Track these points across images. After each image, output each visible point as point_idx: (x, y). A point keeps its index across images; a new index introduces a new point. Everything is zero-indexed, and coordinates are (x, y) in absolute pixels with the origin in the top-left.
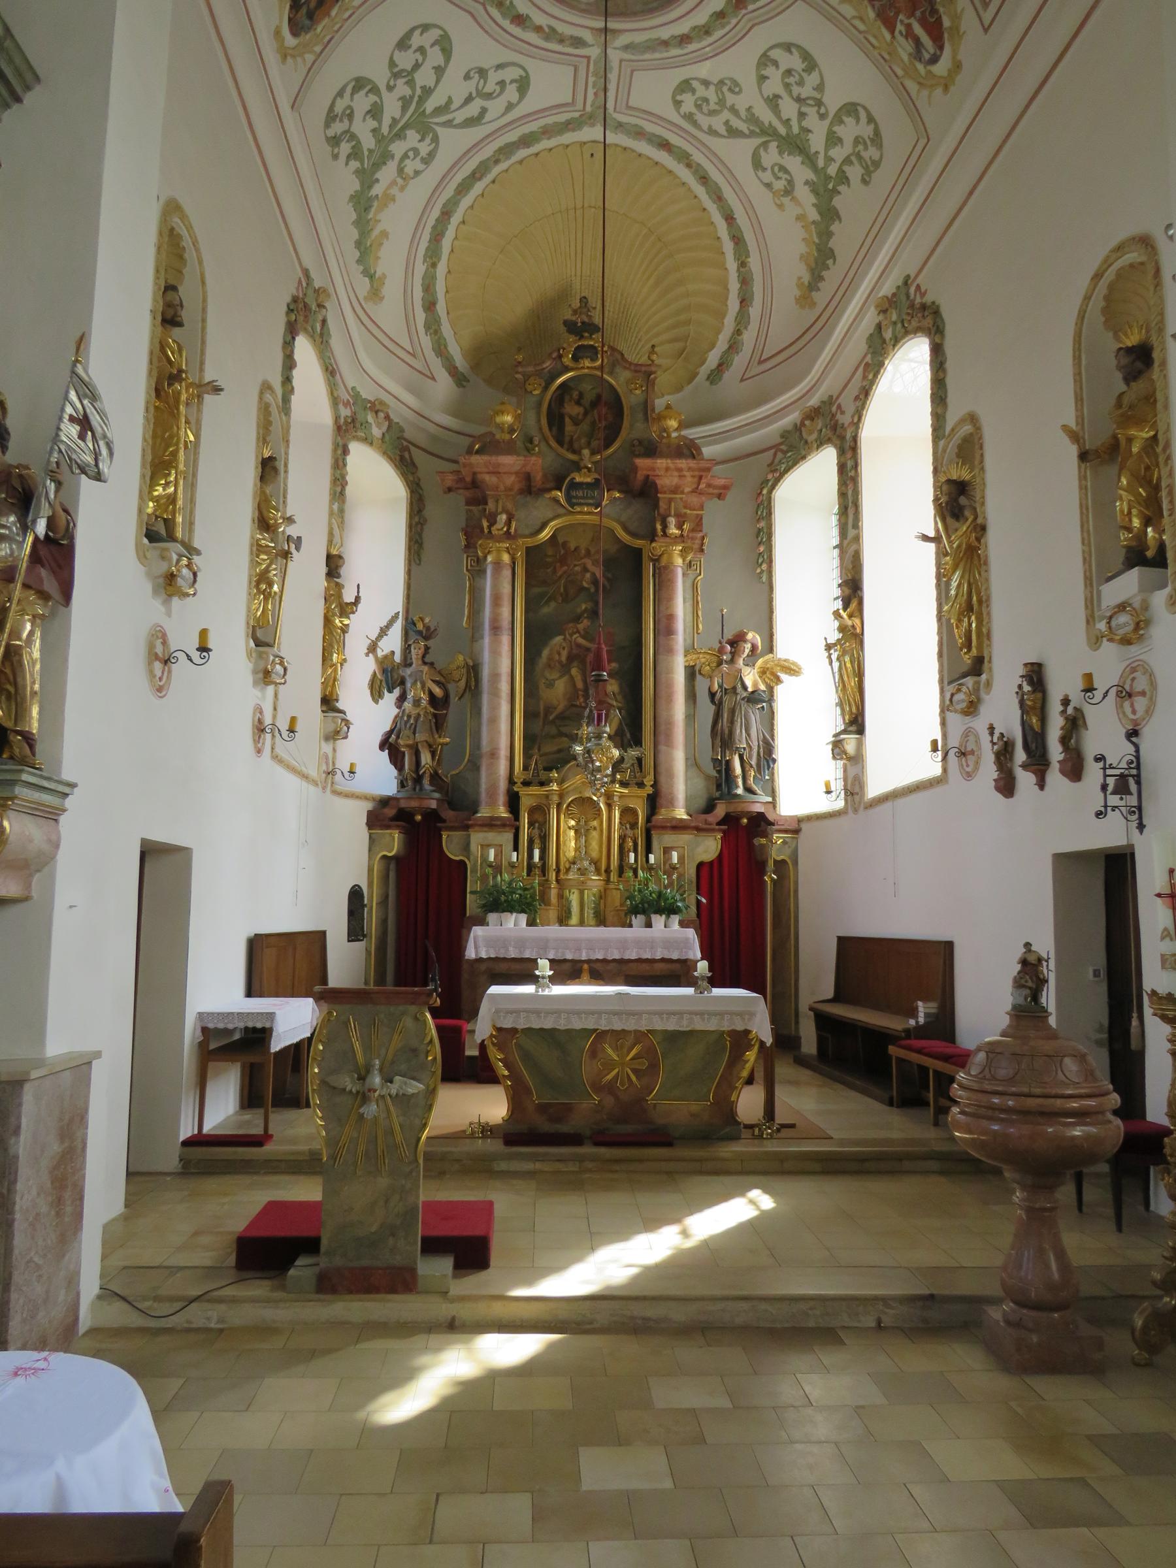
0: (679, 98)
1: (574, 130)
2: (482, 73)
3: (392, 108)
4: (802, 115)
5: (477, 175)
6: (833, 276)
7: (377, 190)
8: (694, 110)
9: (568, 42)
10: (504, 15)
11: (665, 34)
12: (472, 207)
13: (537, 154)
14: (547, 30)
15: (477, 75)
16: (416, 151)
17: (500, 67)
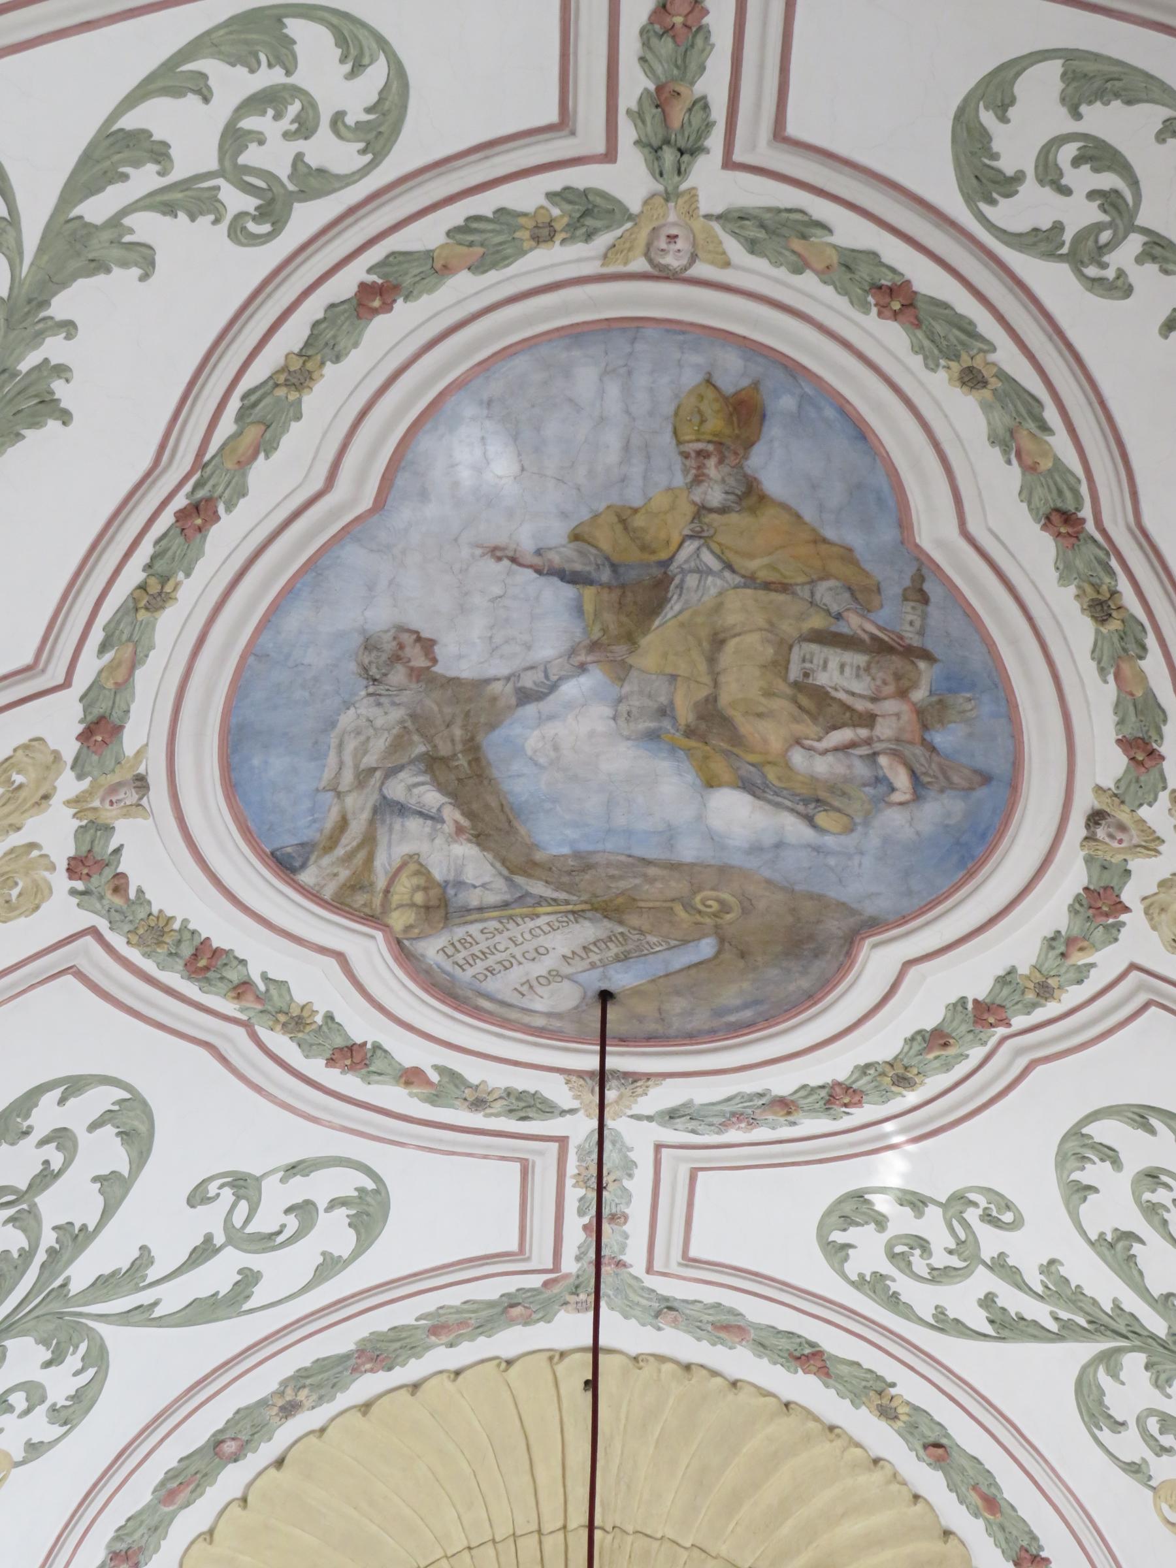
0: (838, 1237)
1: (527, 1321)
5: (229, 1447)
8: (887, 1268)
9: (498, 1106)
10: (307, 1049)
11: (782, 1082)
12: (209, 1535)
13: (415, 1387)
14: (434, 1077)
15: (228, 1195)
16: (35, 1393)
17: (293, 1169)
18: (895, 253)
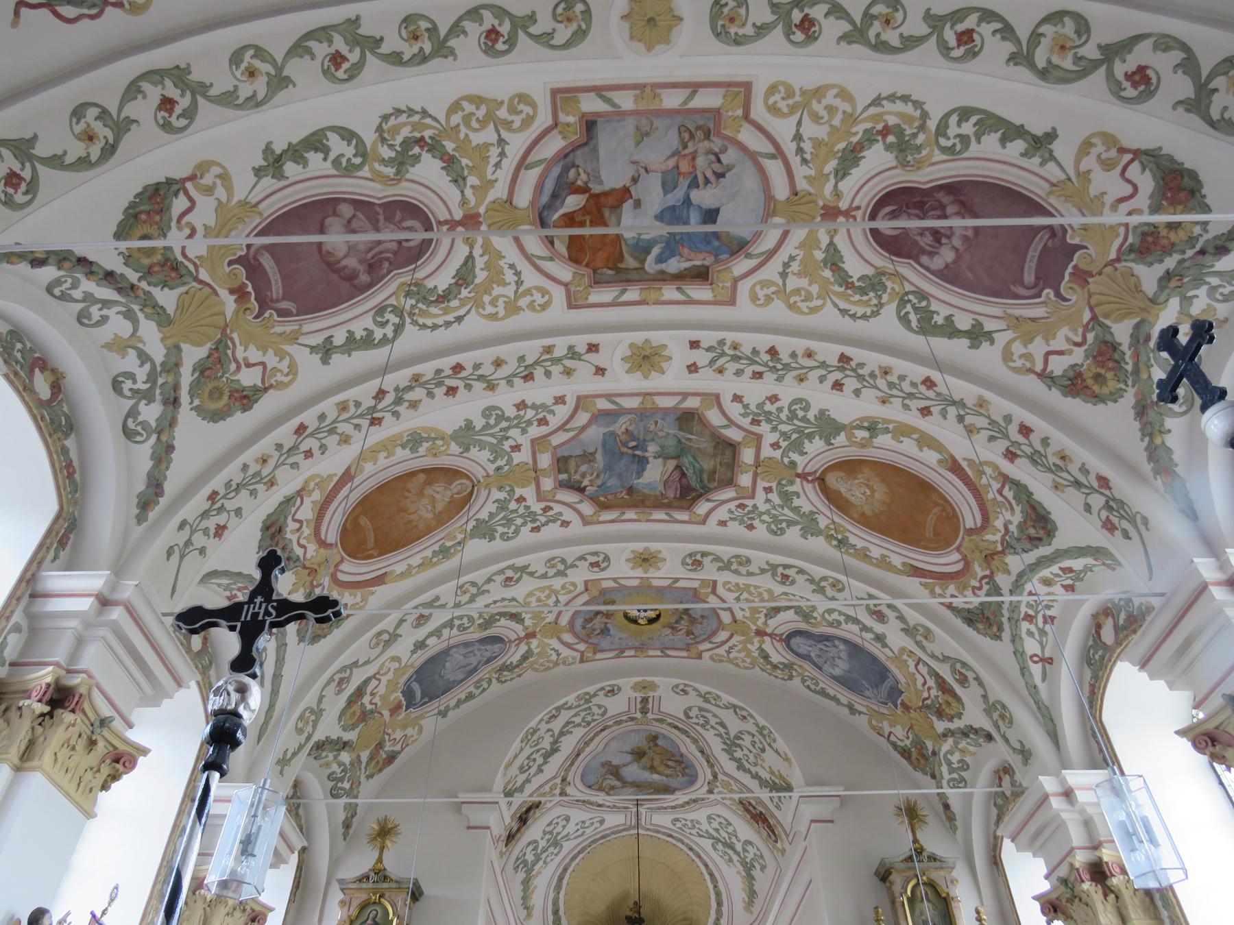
2: (583, 822)
3: (542, 844)
4: (730, 838)
6: (758, 903)
7: (534, 873)
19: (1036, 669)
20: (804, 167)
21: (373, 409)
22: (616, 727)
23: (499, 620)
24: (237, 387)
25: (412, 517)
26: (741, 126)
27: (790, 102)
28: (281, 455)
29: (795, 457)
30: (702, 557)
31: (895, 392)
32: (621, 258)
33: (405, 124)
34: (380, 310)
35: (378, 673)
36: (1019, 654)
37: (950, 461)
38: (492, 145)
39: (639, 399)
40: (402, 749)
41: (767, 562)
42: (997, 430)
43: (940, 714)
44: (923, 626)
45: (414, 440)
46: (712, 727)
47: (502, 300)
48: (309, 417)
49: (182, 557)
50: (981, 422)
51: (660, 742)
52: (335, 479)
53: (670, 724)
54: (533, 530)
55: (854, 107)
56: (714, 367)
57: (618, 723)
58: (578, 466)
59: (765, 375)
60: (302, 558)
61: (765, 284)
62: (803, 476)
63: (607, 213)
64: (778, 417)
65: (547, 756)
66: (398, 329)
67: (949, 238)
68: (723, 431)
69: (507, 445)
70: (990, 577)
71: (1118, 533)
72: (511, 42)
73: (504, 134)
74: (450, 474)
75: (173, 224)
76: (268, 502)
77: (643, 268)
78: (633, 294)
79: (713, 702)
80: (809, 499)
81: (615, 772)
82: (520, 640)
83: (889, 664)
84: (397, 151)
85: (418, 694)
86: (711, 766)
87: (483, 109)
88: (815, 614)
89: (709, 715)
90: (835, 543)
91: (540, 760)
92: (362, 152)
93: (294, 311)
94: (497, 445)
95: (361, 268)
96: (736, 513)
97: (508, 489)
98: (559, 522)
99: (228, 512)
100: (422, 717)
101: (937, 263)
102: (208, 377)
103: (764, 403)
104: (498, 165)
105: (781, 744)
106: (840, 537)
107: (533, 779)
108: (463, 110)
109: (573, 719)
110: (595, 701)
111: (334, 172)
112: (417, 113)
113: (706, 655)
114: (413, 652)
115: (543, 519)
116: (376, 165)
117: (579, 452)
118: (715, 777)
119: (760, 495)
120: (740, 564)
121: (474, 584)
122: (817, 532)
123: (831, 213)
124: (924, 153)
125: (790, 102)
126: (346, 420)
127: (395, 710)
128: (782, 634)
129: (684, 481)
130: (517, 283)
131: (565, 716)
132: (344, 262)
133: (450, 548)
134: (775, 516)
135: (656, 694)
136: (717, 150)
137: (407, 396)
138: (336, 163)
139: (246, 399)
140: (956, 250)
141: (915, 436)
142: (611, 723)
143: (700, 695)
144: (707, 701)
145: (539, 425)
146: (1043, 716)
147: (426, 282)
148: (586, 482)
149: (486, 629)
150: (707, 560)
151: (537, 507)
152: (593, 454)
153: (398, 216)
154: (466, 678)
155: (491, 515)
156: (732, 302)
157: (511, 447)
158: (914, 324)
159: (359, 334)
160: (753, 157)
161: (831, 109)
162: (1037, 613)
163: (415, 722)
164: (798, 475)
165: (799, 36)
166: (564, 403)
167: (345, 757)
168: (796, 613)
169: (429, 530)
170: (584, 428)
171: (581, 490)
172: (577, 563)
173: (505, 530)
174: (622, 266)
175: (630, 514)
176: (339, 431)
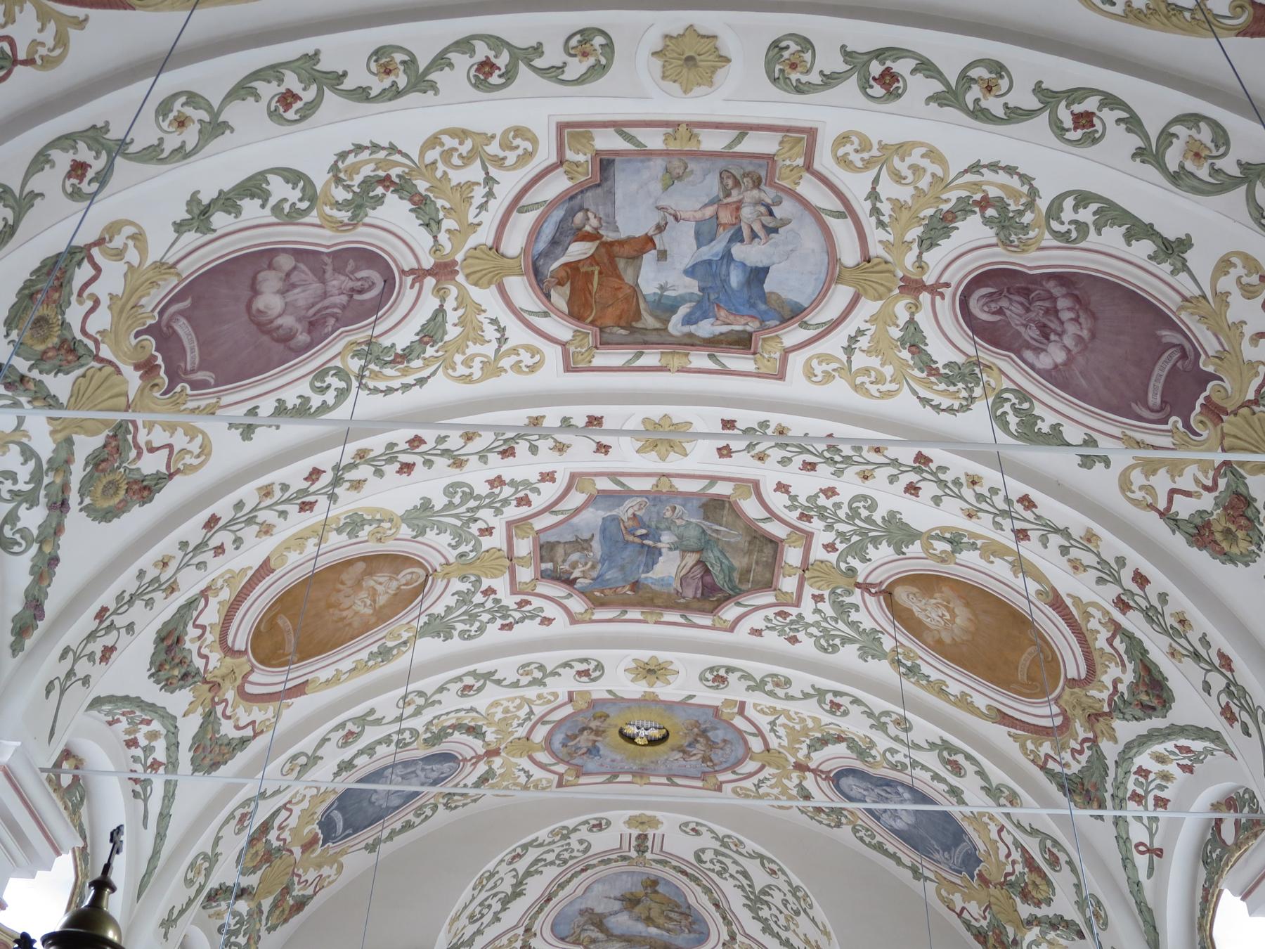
18: (683, 867)
19: (1141, 861)
20: (880, 230)
21: (305, 492)
22: (602, 867)
23: (452, 734)
24: (137, 477)
25: (345, 613)
26: (801, 177)
27: (866, 155)
28: (187, 554)
29: (855, 563)
30: (727, 672)
31: (984, 506)
32: (638, 315)
33: (367, 162)
34: (321, 374)
35: (290, 802)
36: (1123, 840)
37: (1051, 594)
38: (478, 184)
39: (653, 480)
40: (315, 893)
41: (813, 686)
42: (1108, 572)
43: (1025, 896)
44: (1009, 788)
45: (354, 523)
46: (731, 876)
47: (478, 360)
48: (223, 507)
49: (62, 692)
50: (1088, 559)
51: (660, 888)
52: (250, 573)
53: (675, 868)
54: (503, 627)
55: (946, 168)
56: (753, 453)
57: (603, 862)
58: (567, 555)
59: (818, 467)
60: (202, 671)
61: (824, 358)
62: (865, 587)
63: (621, 264)
64: (835, 514)
65: (506, 902)
66: (342, 394)
67: (1060, 335)
68: (761, 525)
69: (474, 529)
70: (1094, 742)
71: (1237, 725)
72: (509, 75)
73: (494, 172)
74: (398, 561)
75: (74, 298)
76: (166, 609)
77: (666, 329)
78: (651, 358)
79: (735, 849)
80: (870, 614)
81: (598, 921)
82: (478, 758)
83: (965, 825)
84: (354, 192)
85: (340, 825)
86: (728, 923)
87: (468, 144)
88: (873, 752)
89: (728, 862)
90: (903, 670)
91: (497, 907)
92: (310, 194)
93: (212, 381)
94: (461, 528)
95: (299, 327)
96: (774, 621)
97: (473, 579)
98: (538, 619)
99: (118, 629)
100: (344, 852)
101: (1044, 361)
102: (103, 471)
103: (817, 496)
104: (483, 207)
105: (818, 912)
106: (909, 664)
107: (486, 930)
108: (442, 144)
109: (544, 857)
110: (574, 837)
111: (274, 220)
112: (383, 148)
113: (727, 788)
114: (336, 774)
115: (517, 615)
116: (327, 209)
117: (570, 538)
118: (733, 938)
119: (807, 605)
120: (777, 685)
121: (421, 694)
122: (880, 655)
123: (912, 287)
124: (1032, 234)
125: (866, 155)
126: (269, 507)
127: (308, 846)
128: (830, 771)
129: (708, 579)
130: (499, 340)
131: (533, 854)
132: (279, 321)
133: (391, 649)
134: (825, 630)
135: (659, 832)
136: (769, 201)
137: (348, 476)
138: (277, 209)
139: (145, 489)
140: (1069, 351)
141: (1010, 559)
142: (595, 862)
143: (717, 838)
144: (724, 845)
145: (518, 505)
146: (1145, 921)
147: (381, 340)
148: (576, 574)
149: (433, 745)
150: (732, 678)
151: (510, 601)
152: (589, 541)
153: (351, 264)
154: (404, 803)
155: (449, 609)
156: (780, 376)
157: (480, 530)
158: (1013, 427)
159: (292, 401)
160: (816, 213)
161: (915, 169)
162: (1147, 792)
163: (334, 860)
164: (858, 585)
165: (878, 91)
166: (553, 480)
167: (243, 906)
168: (849, 747)
169: (366, 628)
170: (578, 511)
171: (571, 582)
172: (560, 670)
173: (467, 627)
174: (639, 325)
175: (634, 614)
176: (259, 520)
